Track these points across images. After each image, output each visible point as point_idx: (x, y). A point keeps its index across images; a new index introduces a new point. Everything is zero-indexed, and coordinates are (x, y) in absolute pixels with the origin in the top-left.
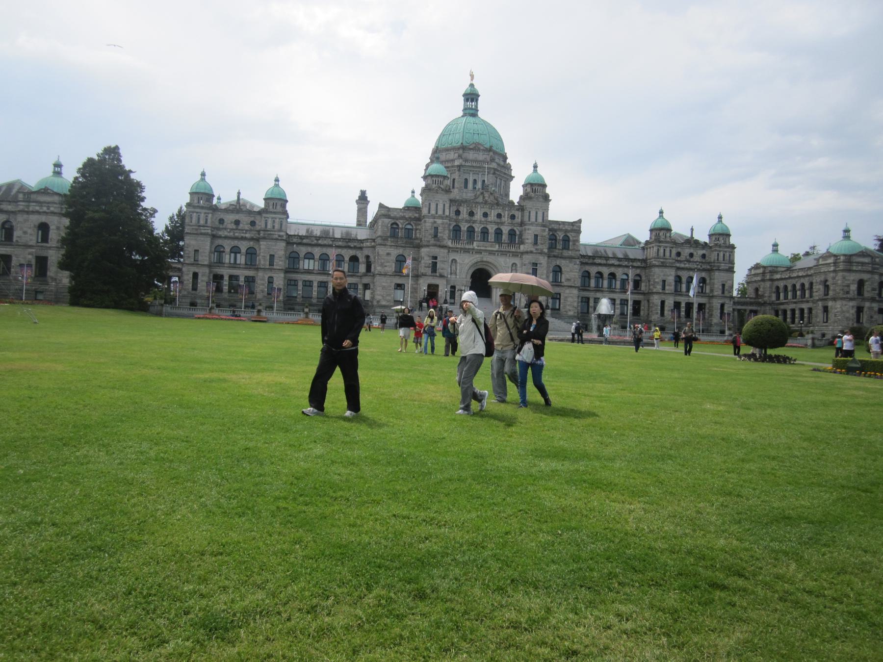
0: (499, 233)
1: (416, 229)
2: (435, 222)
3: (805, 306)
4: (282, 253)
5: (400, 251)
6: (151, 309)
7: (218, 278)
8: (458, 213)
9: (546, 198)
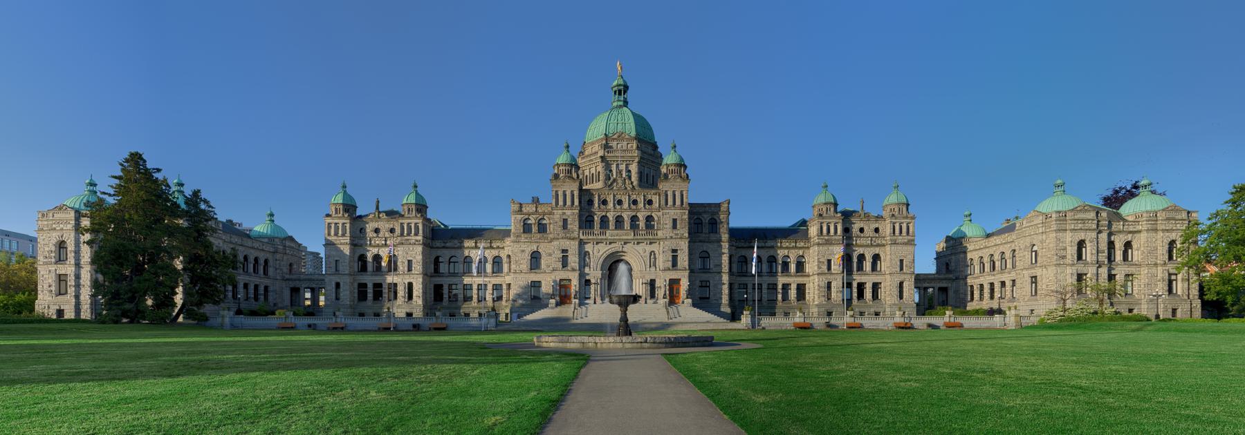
0: (634, 219)
3: (1007, 278)
4: (420, 257)
6: (211, 322)
7: (362, 286)
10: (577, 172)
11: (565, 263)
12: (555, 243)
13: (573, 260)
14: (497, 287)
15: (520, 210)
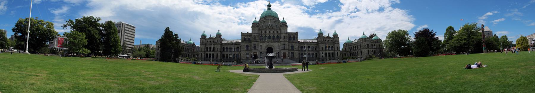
0: (274, 36)
5: (247, 44)
7: (207, 54)
8: (262, 32)
9: (287, 26)
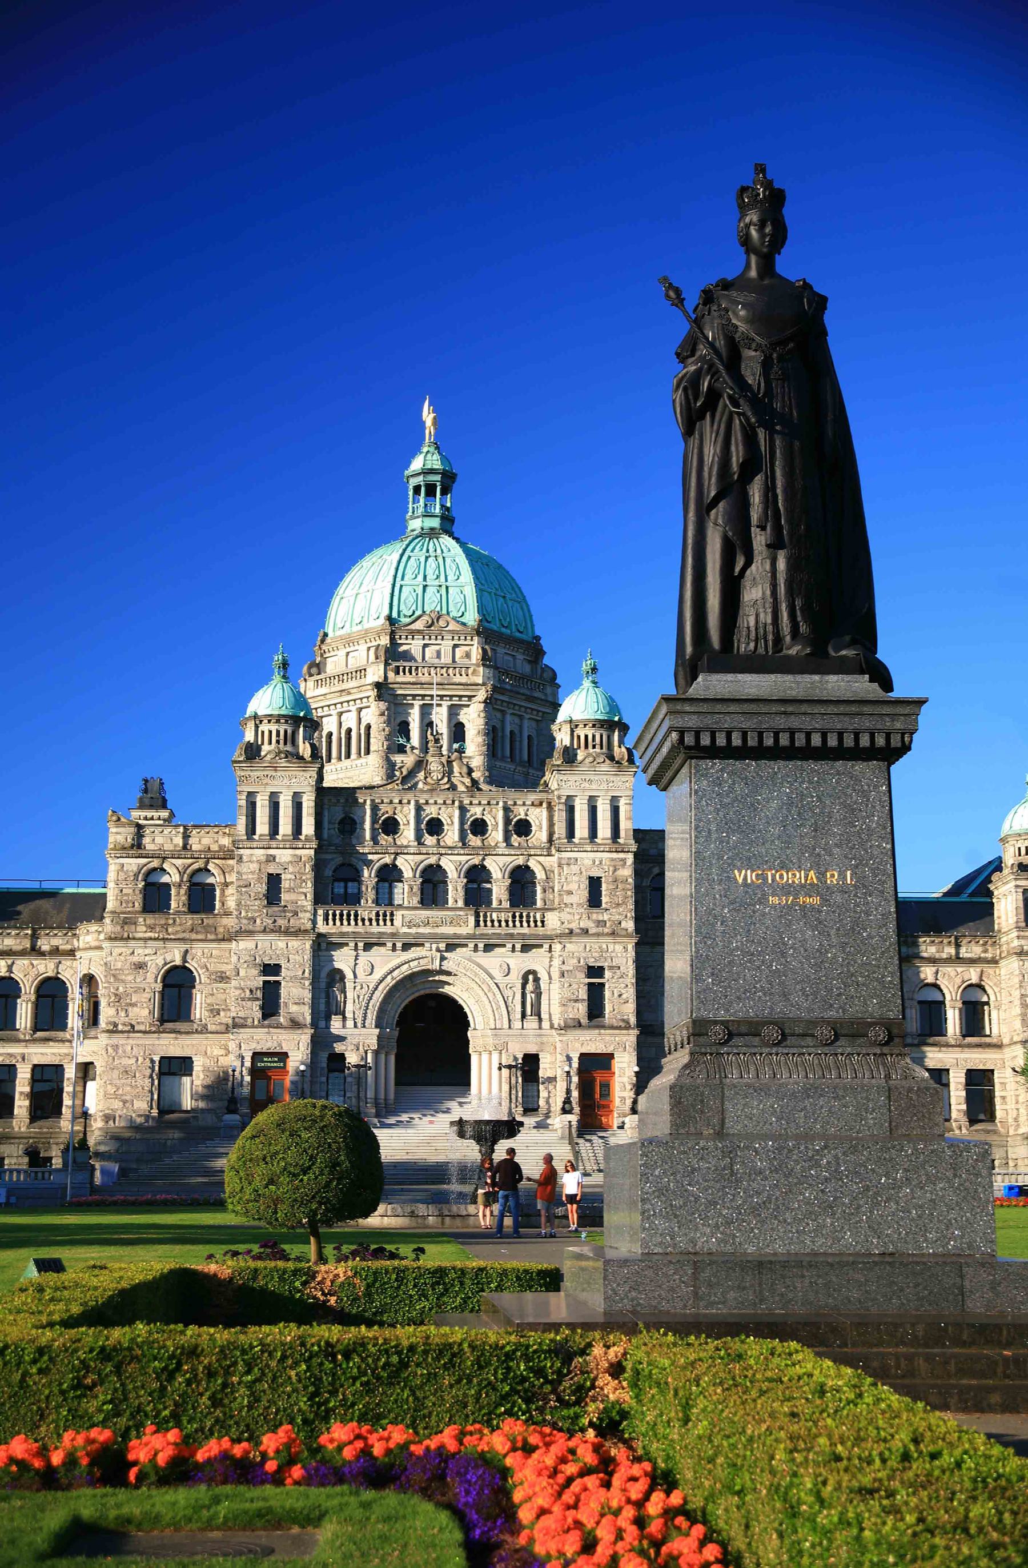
1: (226, 885)
2: (271, 859)
10: (308, 738)
11: (270, 1001)
12: (245, 945)
13: (296, 995)
14: (48, 1077)
15: (137, 844)
